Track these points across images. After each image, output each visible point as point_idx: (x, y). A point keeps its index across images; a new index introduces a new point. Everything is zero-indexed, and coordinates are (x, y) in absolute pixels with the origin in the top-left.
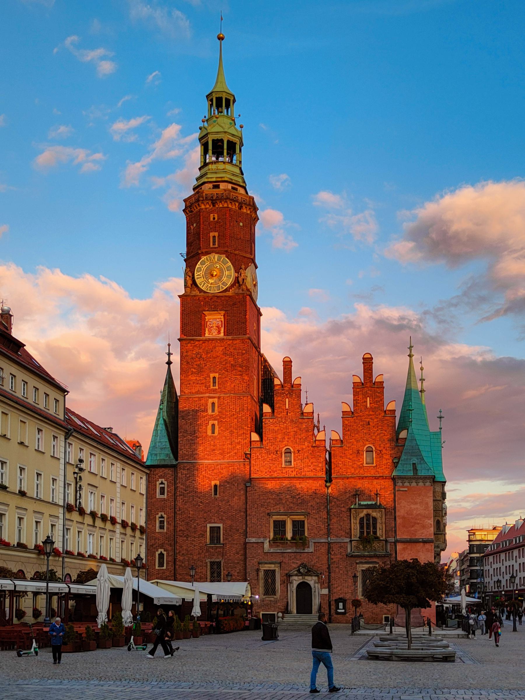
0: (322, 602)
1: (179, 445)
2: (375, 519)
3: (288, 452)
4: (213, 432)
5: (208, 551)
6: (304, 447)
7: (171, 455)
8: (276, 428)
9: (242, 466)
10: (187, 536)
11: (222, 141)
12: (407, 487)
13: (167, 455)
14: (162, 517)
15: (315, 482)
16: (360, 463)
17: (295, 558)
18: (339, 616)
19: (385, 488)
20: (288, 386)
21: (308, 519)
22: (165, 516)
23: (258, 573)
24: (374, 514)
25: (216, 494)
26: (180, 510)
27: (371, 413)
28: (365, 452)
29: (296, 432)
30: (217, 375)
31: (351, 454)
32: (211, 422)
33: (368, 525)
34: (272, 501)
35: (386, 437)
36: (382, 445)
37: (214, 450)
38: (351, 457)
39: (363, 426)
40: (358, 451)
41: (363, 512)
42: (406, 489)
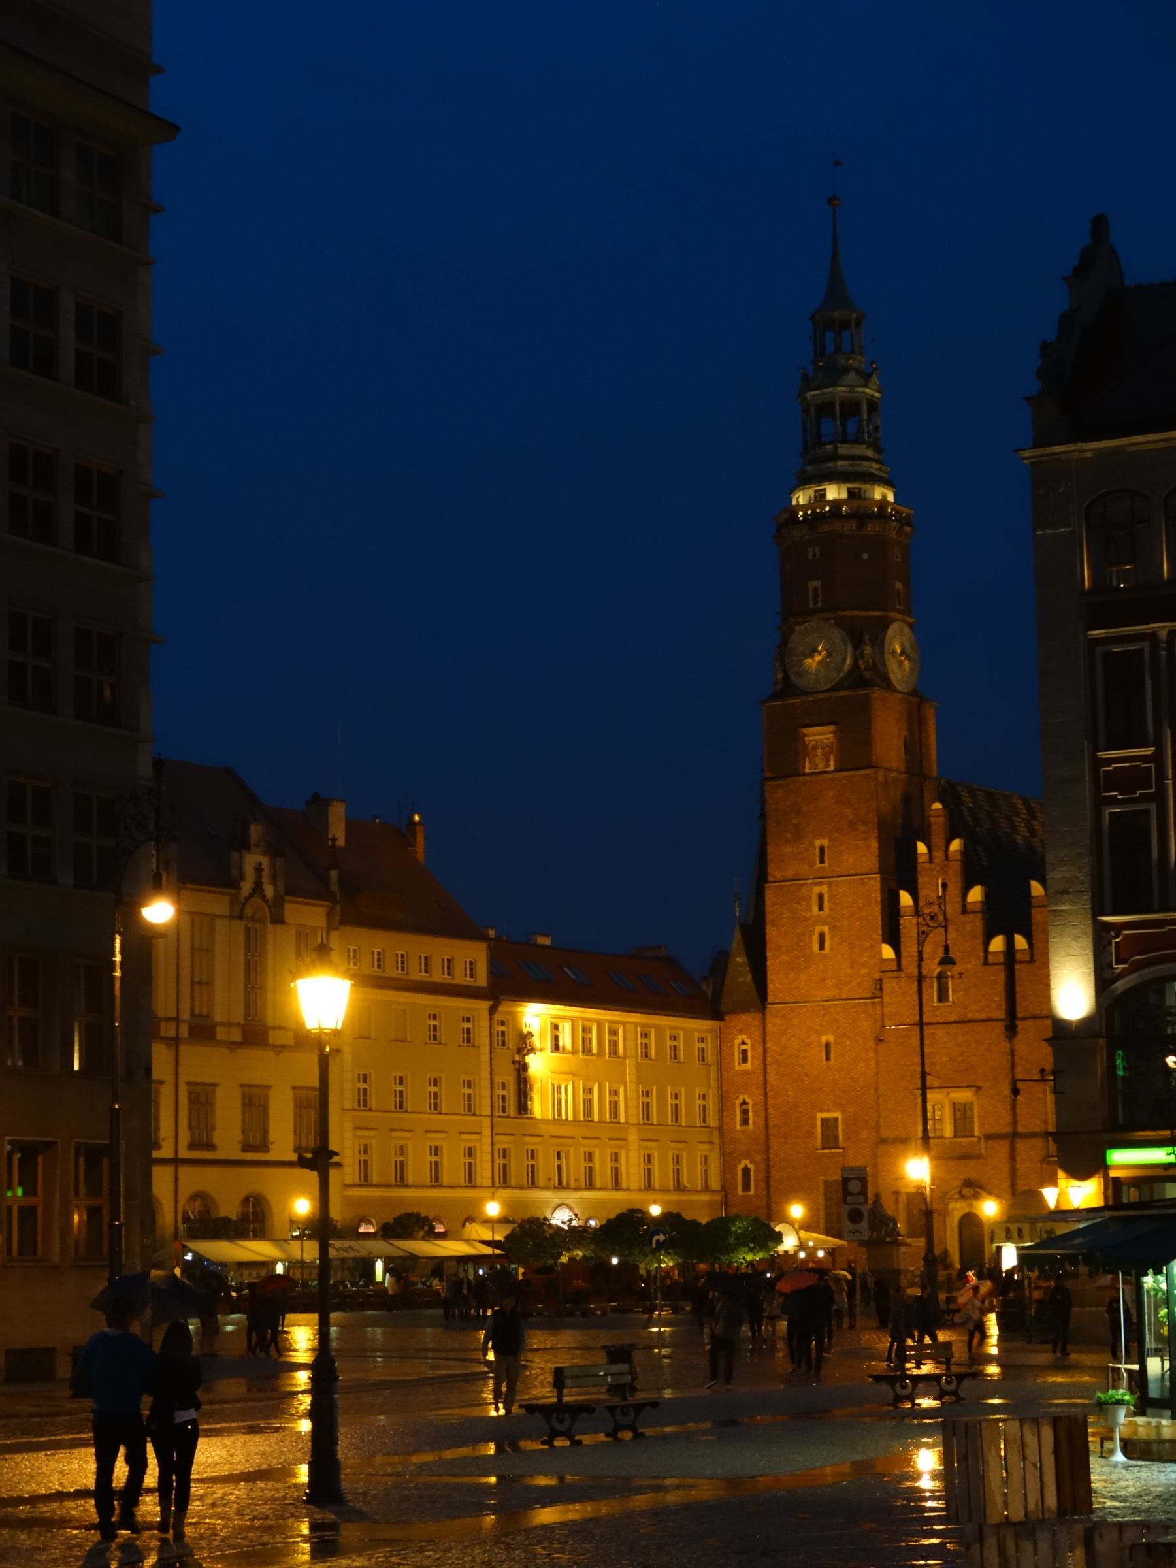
4: (822, 947)
6: (969, 966)
14: (744, 1103)
20: (939, 855)
22: (749, 1100)
25: (828, 1059)
26: (772, 1090)
30: (825, 842)
32: (818, 929)
37: (824, 979)
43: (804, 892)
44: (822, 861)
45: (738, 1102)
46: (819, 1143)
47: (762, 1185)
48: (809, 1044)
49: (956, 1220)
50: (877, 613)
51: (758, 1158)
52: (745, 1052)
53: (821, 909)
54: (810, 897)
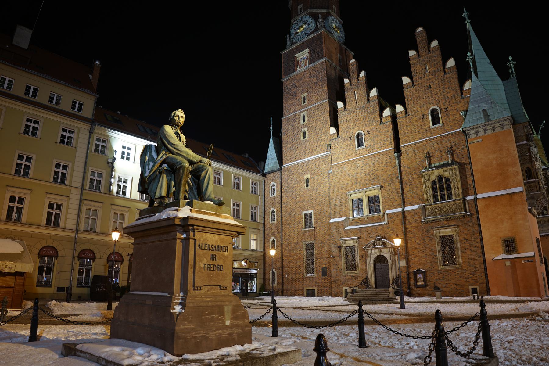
0: (401, 275)
2: (448, 180)
4: (304, 137)
5: (304, 234)
10: (289, 224)
12: (480, 137)
13: (275, 162)
14: (273, 212)
17: (371, 232)
18: (418, 289)
21: (382, 193)
22: (275, 210)
23: (340, 250)
24: (447, 174)
25: (307, 186)
29: (365, 117)
32: (303, 131)
33: (441, 188)
34: (349, 182)
35: (450, 94)
36: (447, 103)
38: (417, 124)
39: (425, 91)
40: (423, 115)
41: (433, 174)
43: (297, 117)
44: (304, 102)
45: (271, 211)
46: (304, 226)
47: (280, 248)
48: (299, 181)
49: (372, 260)
50: (325, 11)
51: (278, 235)
52: (274, 189)
53: (304, 121)
54: (300, 118)
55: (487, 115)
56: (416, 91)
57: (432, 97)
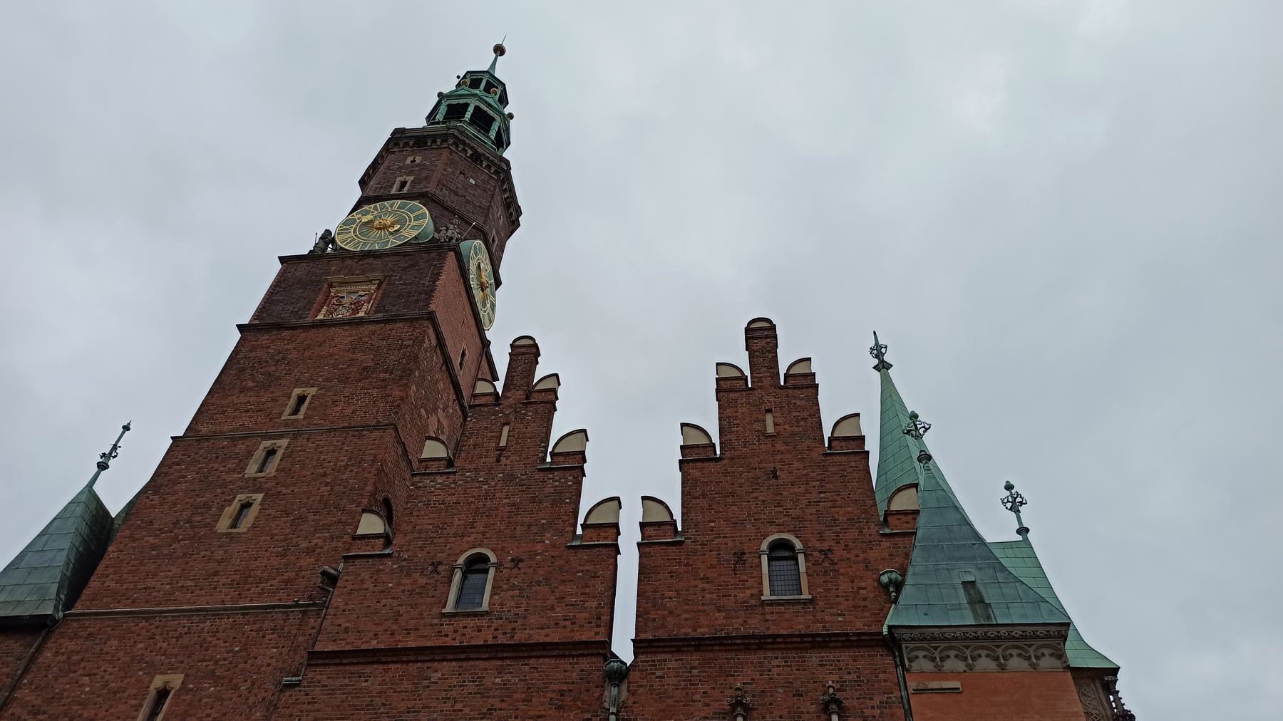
1: (104, 562)
3: (477, 565)
7: (54, 588)
8: (454, 499)
9: (295, 617)
11: (467, 105)
12: (954, 674)
15: (565, 664)
16: (748, 592)
19: (858, 681)
27: (780, 446)
28: (765, 559)
31: (712, 567)
37: (216, 574)
38: (710, 574)
40: (740, 556)
42: (956, 684)
44: (296, 411)
55: (982, 601)
56: (726, 473)
57: (779, 505)
